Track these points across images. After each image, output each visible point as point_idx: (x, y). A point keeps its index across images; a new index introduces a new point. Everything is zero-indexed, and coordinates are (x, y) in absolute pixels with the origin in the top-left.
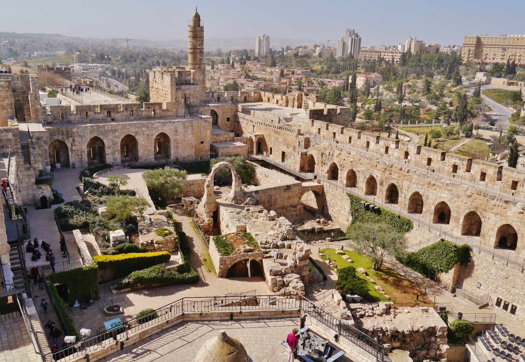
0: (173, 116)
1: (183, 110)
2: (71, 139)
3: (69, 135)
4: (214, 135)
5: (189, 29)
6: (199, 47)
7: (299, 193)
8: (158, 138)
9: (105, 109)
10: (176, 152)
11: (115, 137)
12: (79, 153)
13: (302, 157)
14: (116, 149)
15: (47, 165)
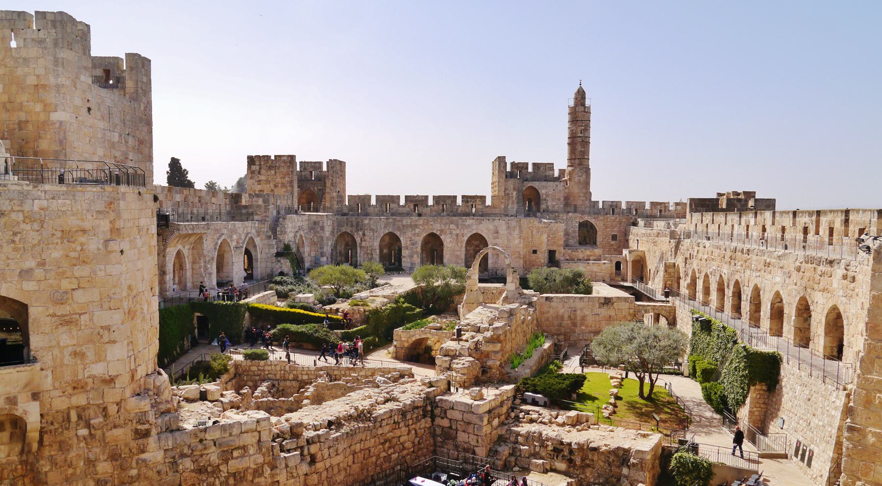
0: (500, 214)
1: (516, 206)
2: (361, 233)
3: (359, 227)
4: (569, 249)
5: (567, 111)
6: (581, 135)
7: (630, 314)
8: (476, 243)
9: (411, 201)
10: (496, 263)
11: (414, 234)
12: (369, 251)
13: (666, 271)
14: (415, 250)
15: (323, 256)
